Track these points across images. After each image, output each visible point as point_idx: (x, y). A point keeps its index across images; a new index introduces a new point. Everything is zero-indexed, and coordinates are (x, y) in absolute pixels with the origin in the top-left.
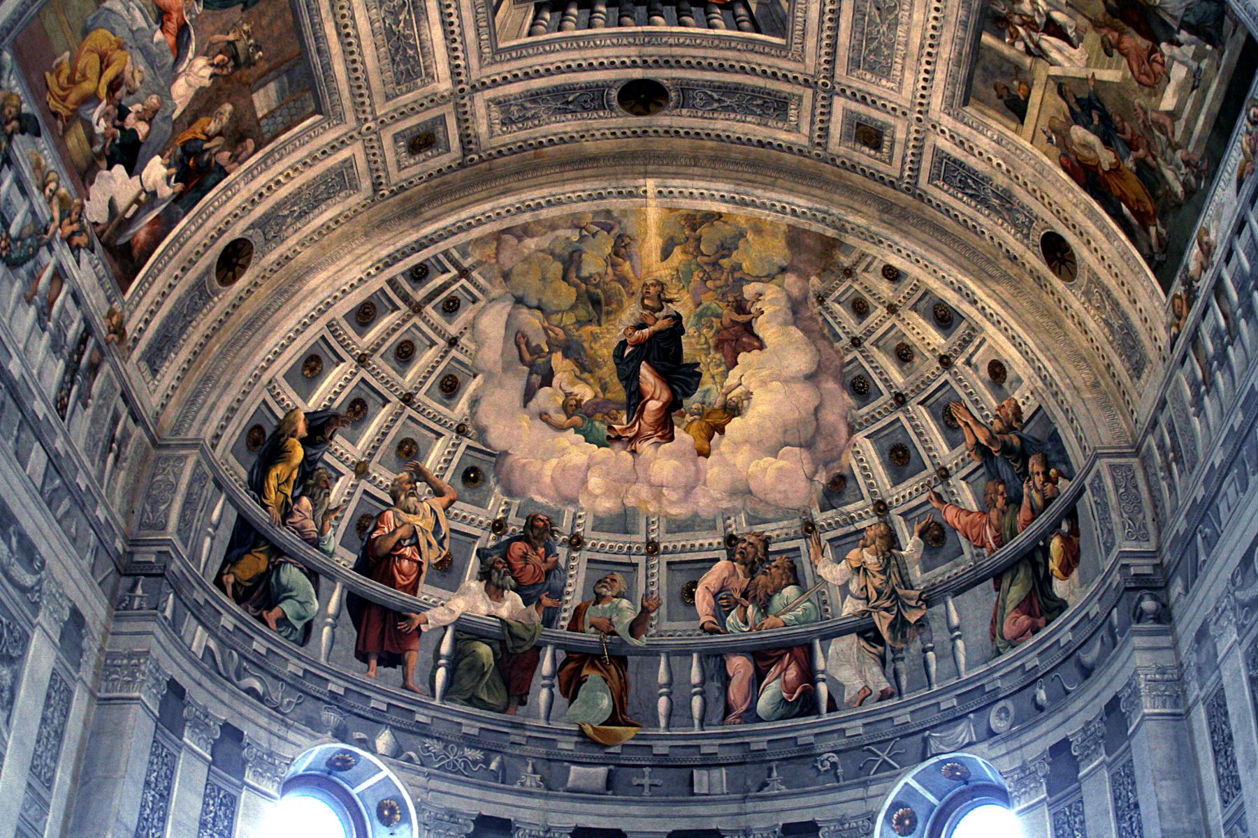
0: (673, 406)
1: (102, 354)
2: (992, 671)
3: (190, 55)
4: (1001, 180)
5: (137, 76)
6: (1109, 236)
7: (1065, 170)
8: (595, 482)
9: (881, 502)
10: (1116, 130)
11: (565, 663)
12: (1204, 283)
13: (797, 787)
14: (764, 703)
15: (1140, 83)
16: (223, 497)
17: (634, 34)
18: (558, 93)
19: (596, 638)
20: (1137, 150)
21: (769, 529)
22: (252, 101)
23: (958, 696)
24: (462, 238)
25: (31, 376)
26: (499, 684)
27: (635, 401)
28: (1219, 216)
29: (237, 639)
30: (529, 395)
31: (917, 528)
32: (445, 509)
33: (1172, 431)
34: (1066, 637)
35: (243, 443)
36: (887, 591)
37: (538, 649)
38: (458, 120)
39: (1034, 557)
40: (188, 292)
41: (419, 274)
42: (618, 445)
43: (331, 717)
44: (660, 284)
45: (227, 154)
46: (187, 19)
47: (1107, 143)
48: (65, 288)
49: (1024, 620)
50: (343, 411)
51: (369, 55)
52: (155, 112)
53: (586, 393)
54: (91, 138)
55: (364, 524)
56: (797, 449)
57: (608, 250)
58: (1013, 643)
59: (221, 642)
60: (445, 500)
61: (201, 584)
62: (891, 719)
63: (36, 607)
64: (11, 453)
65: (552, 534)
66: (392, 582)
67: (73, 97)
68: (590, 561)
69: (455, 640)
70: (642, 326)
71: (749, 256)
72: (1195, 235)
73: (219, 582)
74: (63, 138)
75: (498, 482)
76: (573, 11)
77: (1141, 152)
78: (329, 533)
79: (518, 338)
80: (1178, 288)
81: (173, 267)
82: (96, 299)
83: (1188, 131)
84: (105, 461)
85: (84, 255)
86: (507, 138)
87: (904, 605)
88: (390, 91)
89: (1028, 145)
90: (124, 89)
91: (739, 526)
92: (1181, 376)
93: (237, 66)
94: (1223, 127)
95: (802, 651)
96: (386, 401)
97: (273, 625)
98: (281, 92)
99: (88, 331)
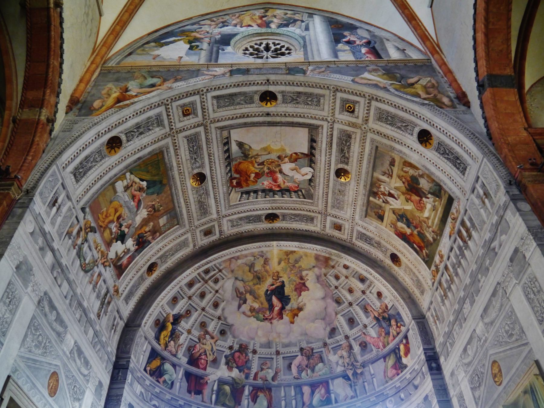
0: (282, 309)
1: (112, 298)
2: (385, 388)
3: (141, 208)
4: (377, 239)
5: (126, 215)
6: (410, 253)
7: (396, 234)
8: (260, 333)
9: (346, 336)
10: (411, 223)
11: (253, 391)
12: (442, 267)
14: (315, 401)
15: (417, 209)
16: (147, 342)
17: (269, 200)
18: (248, 218)
19: (262, 382)
20: (417, 228)
21: (313, 345)
22: (159, 223)
23: (376, 397)
24: (220, 260)
25: (90, 306)
26: (232, 399)
27: (271, 307)
28: (444, 247)
29: (151, 388)
30: (239, 307)
31: (358, 343)
32: (215, 343)
33: (435, 310)
34: (408, 376)
35: (153, 325)
36: (350, 363)
37: (244, 387)
38: (219, 226)
39: (395, 351)
40: (138, 279)
41: (207, 272)
42: (266, 321)
44: (278, 272)
45: (151, 237)
46: (141, 198)
47: (408, 227)
48: (102, 278)
49: (394, 371)
50: (184, 314)
51: (194, 207)
52: (131, 225)
53: (256, 305)
54: (111, 233)
55: (190, 349)
56: (320, 320)
57: (262, 262)
58: (391, 379)
59: (146, 389)
60: (214, 340)
61: (140, 371)
62: (355, 405)
63: (88, 381)
64: (83, 331)
65: (247, 349)
66: (198, 367)
67: (107, 221)
68: (259, 358)
69: (218, 385)
70: (272, 285)
71: (303, 264)
72: (437, 252)
73: (145, 370)
74: (103, 233)
75: (231, 334)
76: (252, 194)
77: (419, 229)
78: (179, 352)
79: (237, 290)
80: (433, 268)
81: (134, 272)
82: (111, 282)
83: (433, 223)
84: (111, 332)
85: (108, 268)
86: (233, 231)
87: (356, 368)
88: (199, 218)
89: (385, 228)
90: (121, 219)
91: (304, 345)
92: (437, 294)
93: (155, 211)
94: (443, 221)
95: (325, 383)
96: (197, 310)
97: (161, 382)
98: (167, 219)
99: (108, 292)
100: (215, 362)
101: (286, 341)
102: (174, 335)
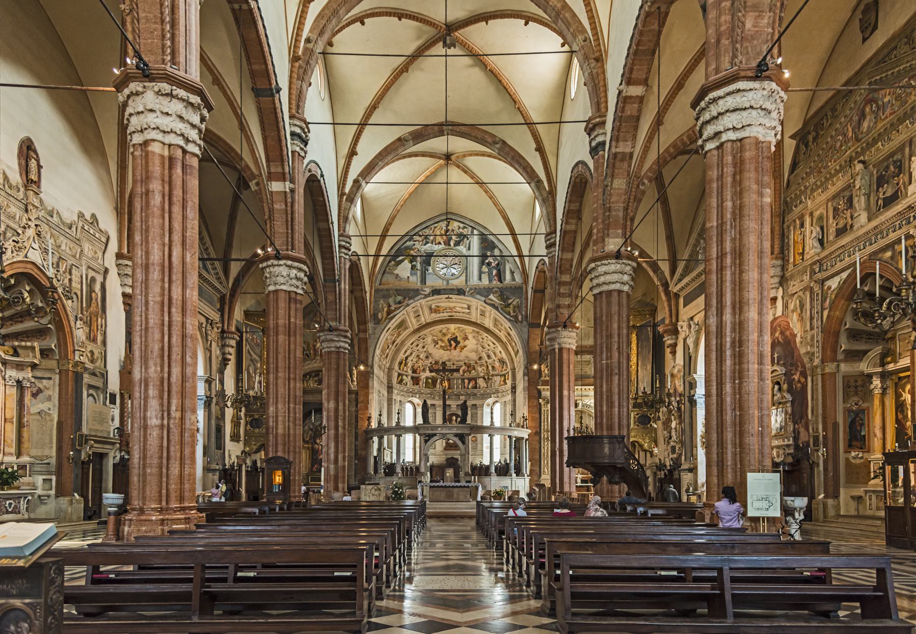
0: (456, 346)
13: (474, 399)
14: (470, 387)
27: (451, 345)
39: (504, 375)
43: (411, 395)
53: (443, 345)
55: (412, 367)
91: (466, 361)
95: (475, 379)
100: (424, 370)
101: (458, 359)
102: (406, 365)
